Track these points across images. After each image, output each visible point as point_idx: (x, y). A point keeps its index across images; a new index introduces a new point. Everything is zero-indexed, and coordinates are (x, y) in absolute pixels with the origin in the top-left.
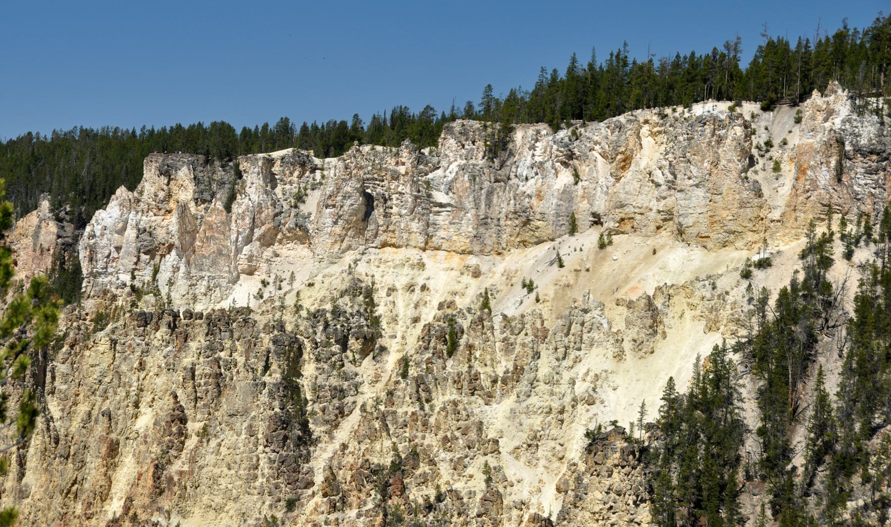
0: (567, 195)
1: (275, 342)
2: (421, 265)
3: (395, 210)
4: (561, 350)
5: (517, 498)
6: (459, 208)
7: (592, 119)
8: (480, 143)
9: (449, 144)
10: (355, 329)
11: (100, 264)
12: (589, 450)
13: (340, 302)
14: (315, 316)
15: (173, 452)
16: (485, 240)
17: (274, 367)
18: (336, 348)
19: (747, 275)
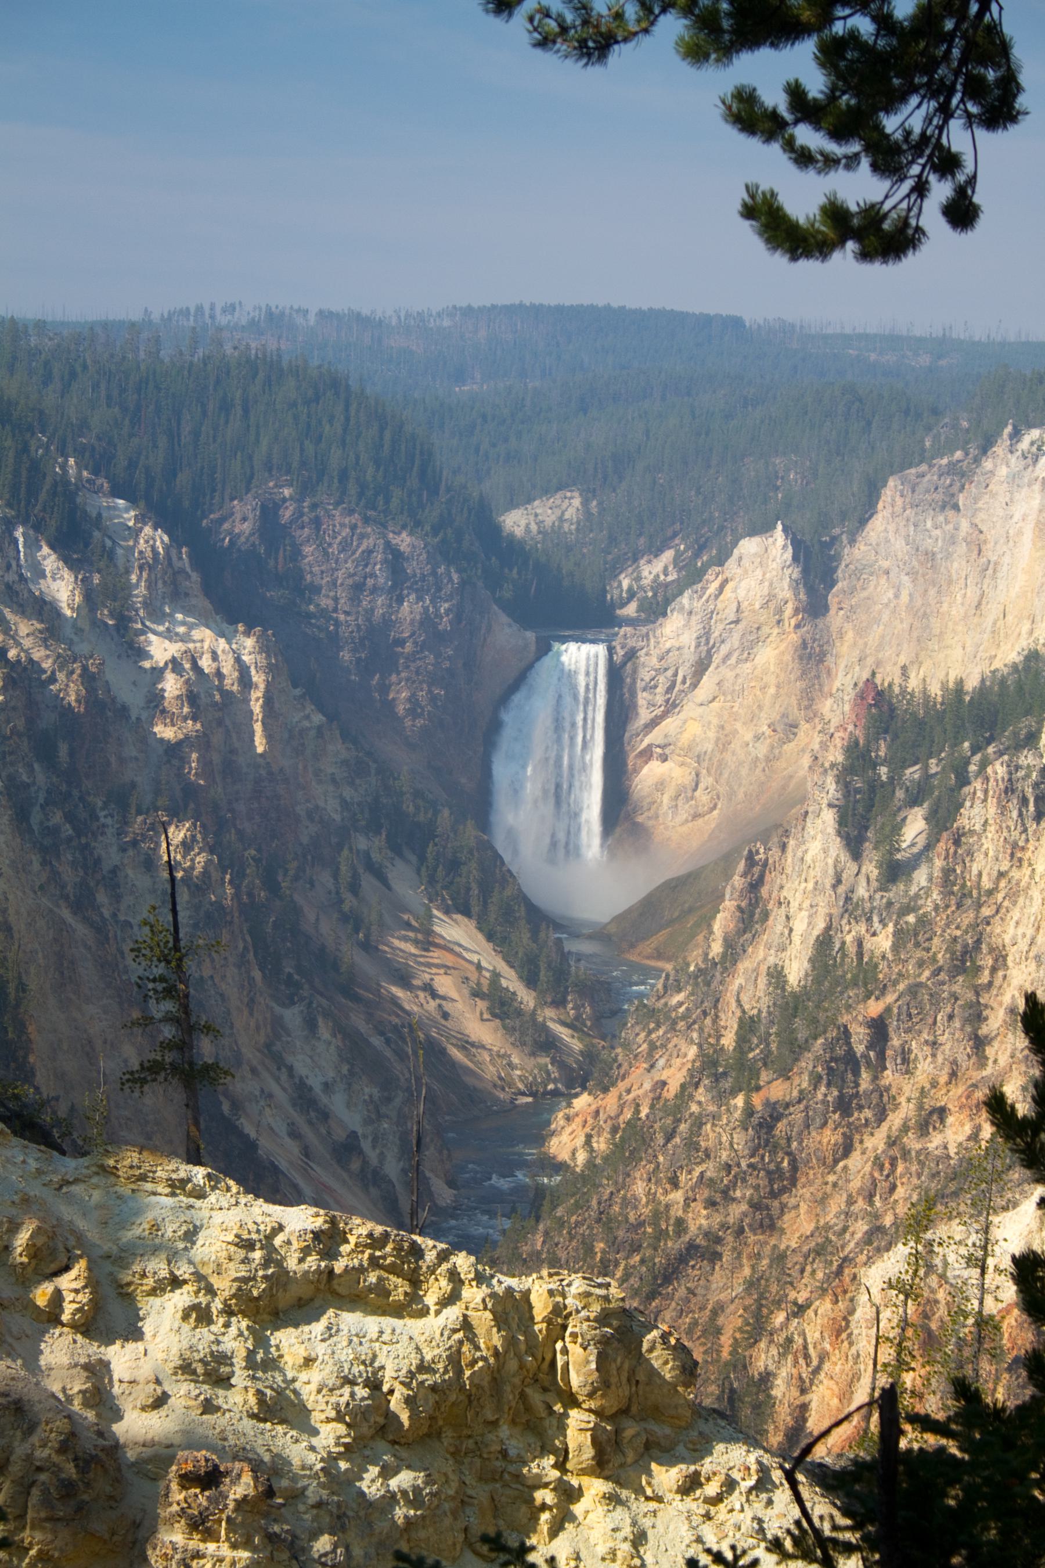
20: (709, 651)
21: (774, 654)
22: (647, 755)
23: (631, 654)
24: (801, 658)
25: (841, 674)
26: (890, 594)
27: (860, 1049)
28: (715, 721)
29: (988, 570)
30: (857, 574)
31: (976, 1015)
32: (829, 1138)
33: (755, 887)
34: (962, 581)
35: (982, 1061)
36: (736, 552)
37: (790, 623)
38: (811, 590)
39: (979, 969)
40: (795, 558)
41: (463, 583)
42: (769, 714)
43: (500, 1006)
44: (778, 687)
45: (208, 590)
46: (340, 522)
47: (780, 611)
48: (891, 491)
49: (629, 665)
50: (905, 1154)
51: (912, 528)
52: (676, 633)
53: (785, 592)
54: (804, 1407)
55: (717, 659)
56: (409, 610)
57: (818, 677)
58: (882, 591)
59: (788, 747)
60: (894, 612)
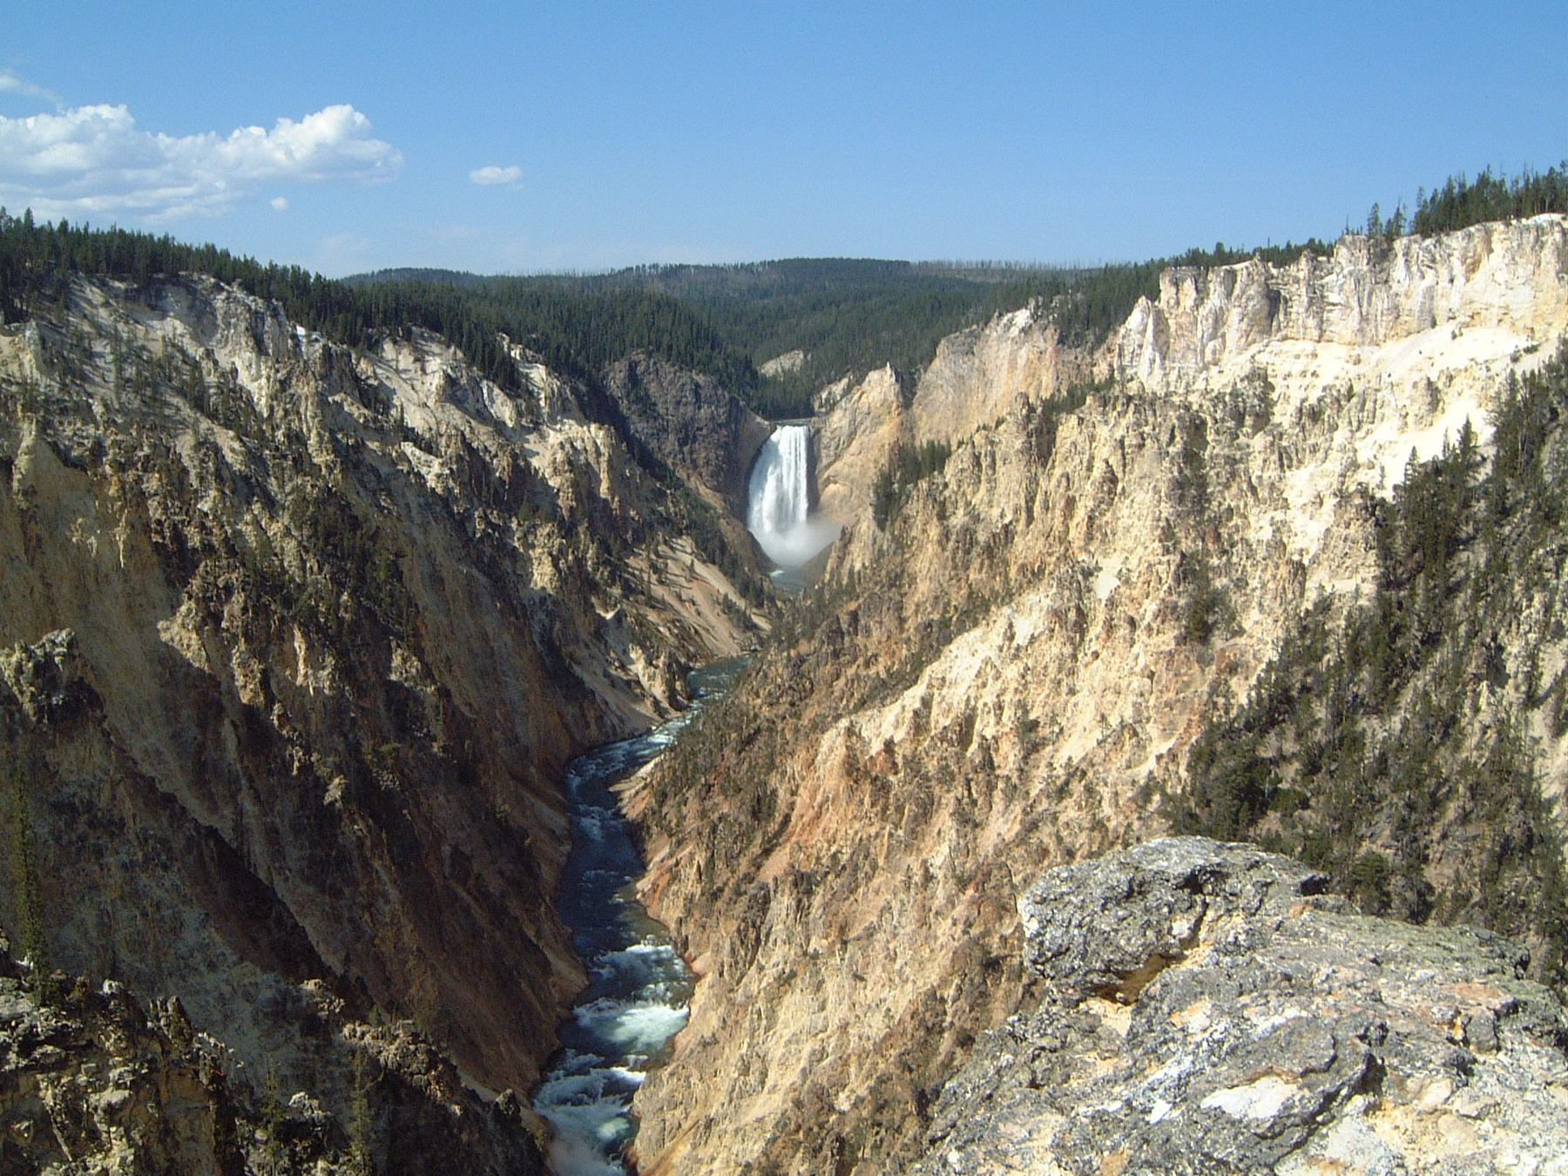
0: (1430, 293)
1: (1179, 418)
2: (1315, 355)
3: (1294, 310)
4: (1355, 424)
5: (1298, 546)
6: (1347, 306)
7: (1455, 229)
8: (1365, 252)
9: (1342, 253)
10: (1252, 407)
11: (1128, 358)
12: (1339, 505)
13: (1239, 386)
14: (1219, 398)
15: (1103, 506)
16: (1365, 333)
17: (1178, 439)
18: (1231, 424)
19: (1515, 359)
22: (828, 481)
23: (818, 431)
27: (844, 627)
29: (988, 384)
30: (927, 387)
31: (900, 608)
32: (828, 669)
33: (845, 546)
35: (902, 630)
37: (895, 413)
38: (905, 397)
39: (900, 586)
41: (732, 399)
43: (728, 607)
45: (582, 407)
46: (668, 369)
48: (942, 348)
50: (858, 676)
54: (793, 803)
56: (704, 412)
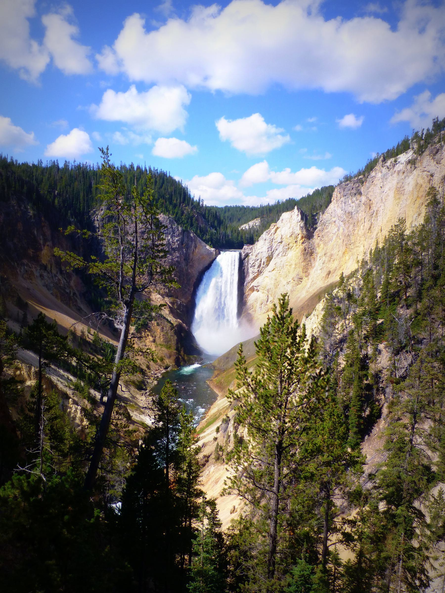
20: (272, 253)
21: (295, 253)
23: (247, 255)
24: (304, 254)
25: (318, 259)
26: (336, 230)
28: (274, 278)
34: (363, 220)
36: (281, 218)
38: (307, 230)
40: (302, 219)
41: (183, 231)
42: (293, 275)
44: (296, 265)
47: (297, 238)
49: (246, 259)
51: (344, 204)
52: (260, 248)
53: (298, 231)
55: (275, 256)
57: (310, 261)
58: (332, 229)
59: (299, 286)
60: (337, 236)
